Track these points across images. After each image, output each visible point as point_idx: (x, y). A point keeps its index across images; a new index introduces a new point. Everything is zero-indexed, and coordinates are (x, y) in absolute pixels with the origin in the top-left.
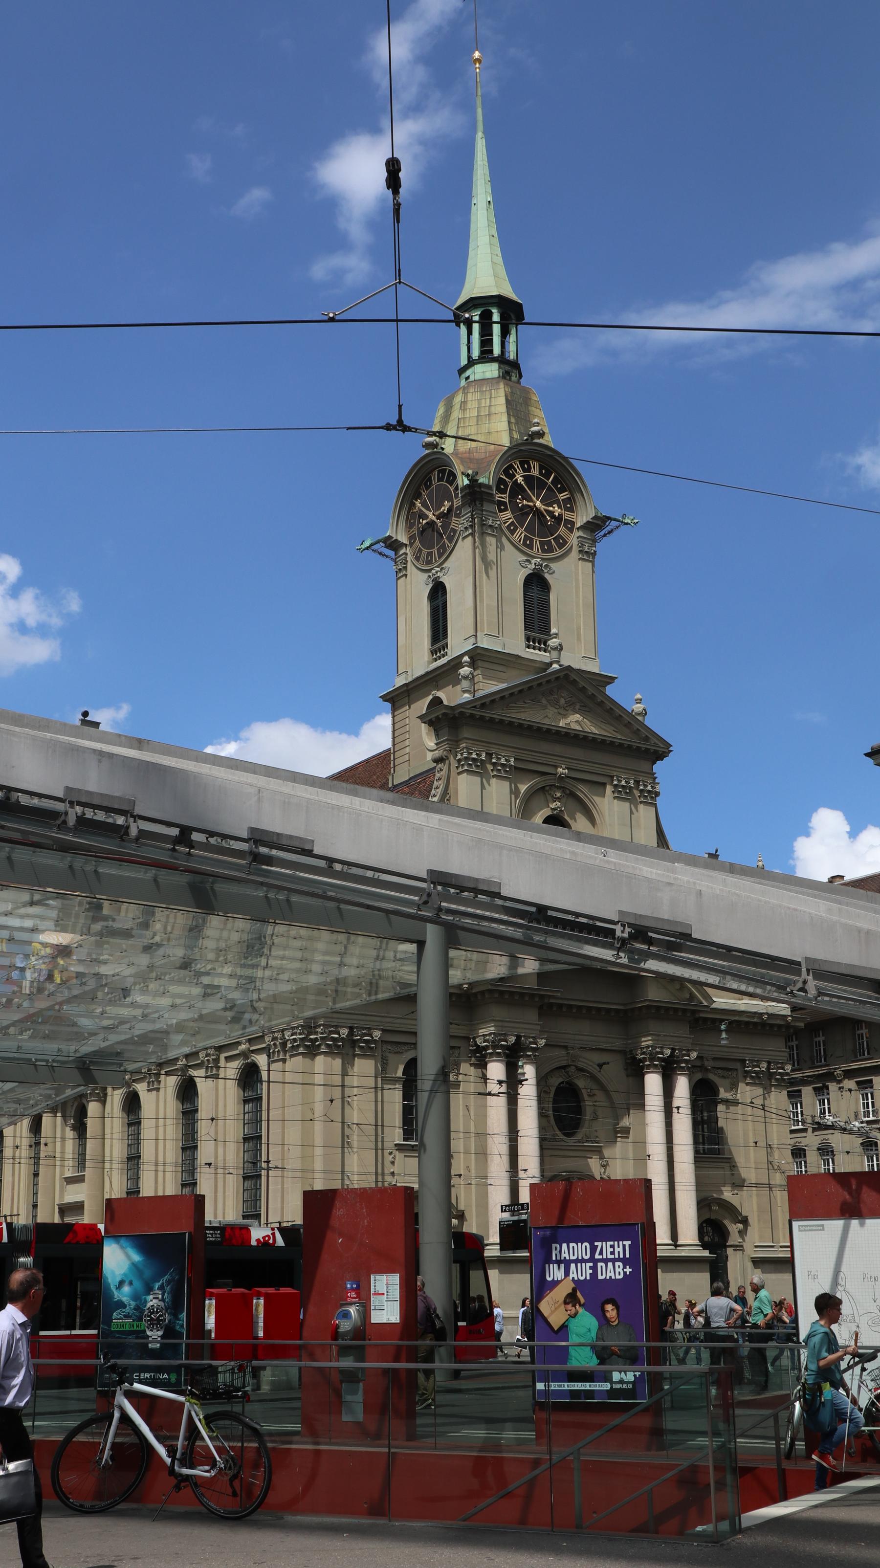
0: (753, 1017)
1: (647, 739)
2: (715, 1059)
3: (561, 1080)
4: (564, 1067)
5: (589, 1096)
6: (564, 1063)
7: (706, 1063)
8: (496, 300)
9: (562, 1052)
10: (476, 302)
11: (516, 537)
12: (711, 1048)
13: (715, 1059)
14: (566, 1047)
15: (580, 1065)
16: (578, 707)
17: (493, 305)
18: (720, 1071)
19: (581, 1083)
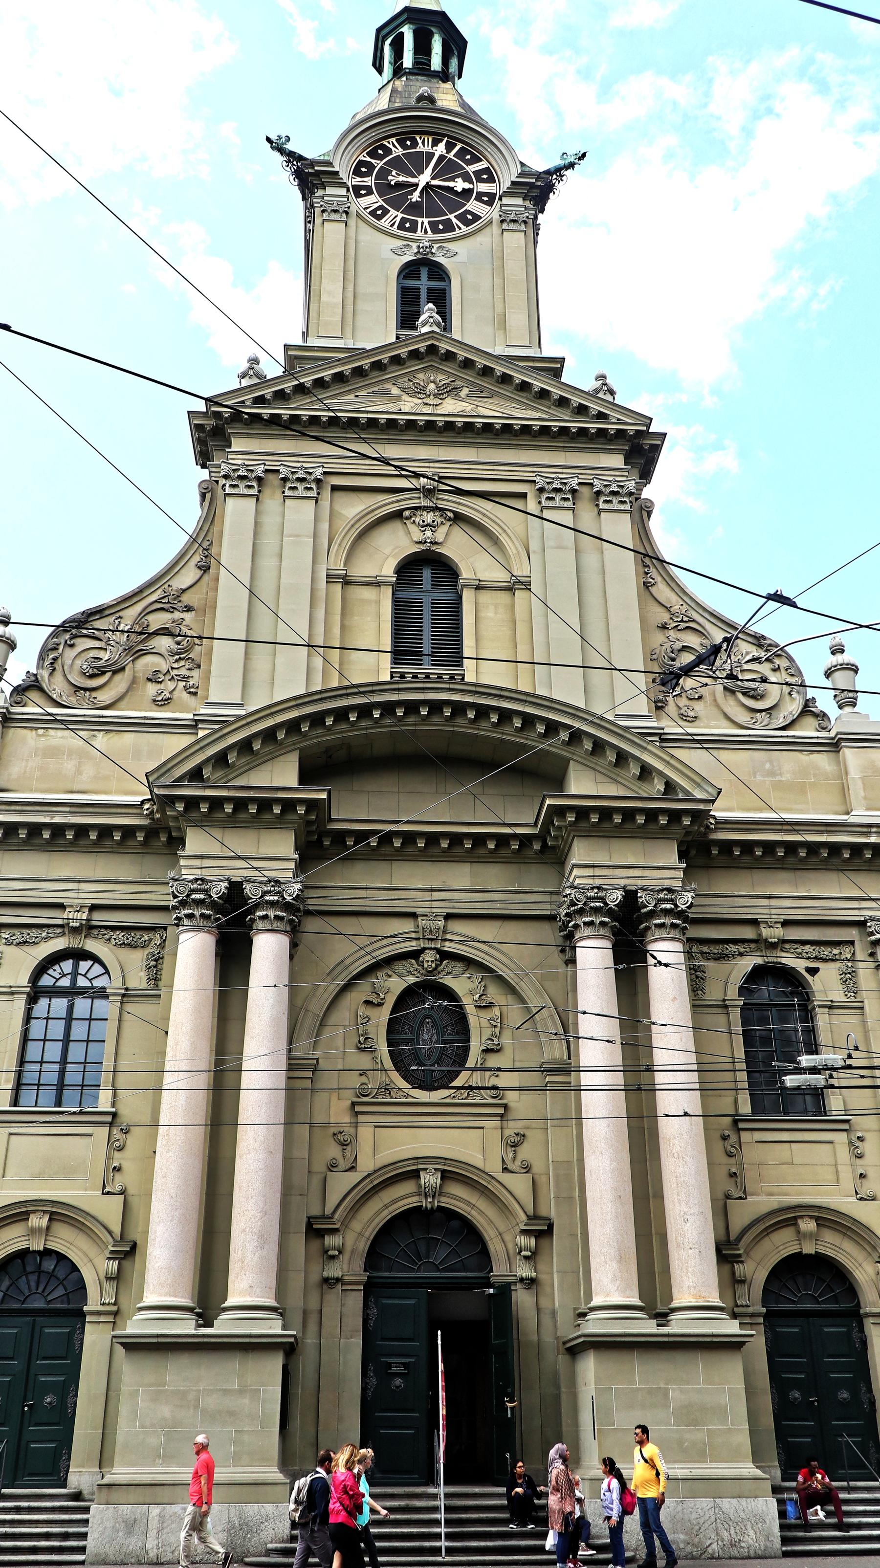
0: (867, 834)
1: (601, 416)
2: (786, 923)
3: (411, 980)
4: (415, 955)
5: (478, 1007)
6: (412, 946)
7: (765, 932)
8: (405, 16)
9: (407, 926)
10: (383, 33)
11: (385, 223)
12: (774, 902)
13: (786, 923)
14: (414, 916)
15: (448, 947)
16: (465, 392)
17: (401, 25)
18: (807, 948)
19: (462, 984)
